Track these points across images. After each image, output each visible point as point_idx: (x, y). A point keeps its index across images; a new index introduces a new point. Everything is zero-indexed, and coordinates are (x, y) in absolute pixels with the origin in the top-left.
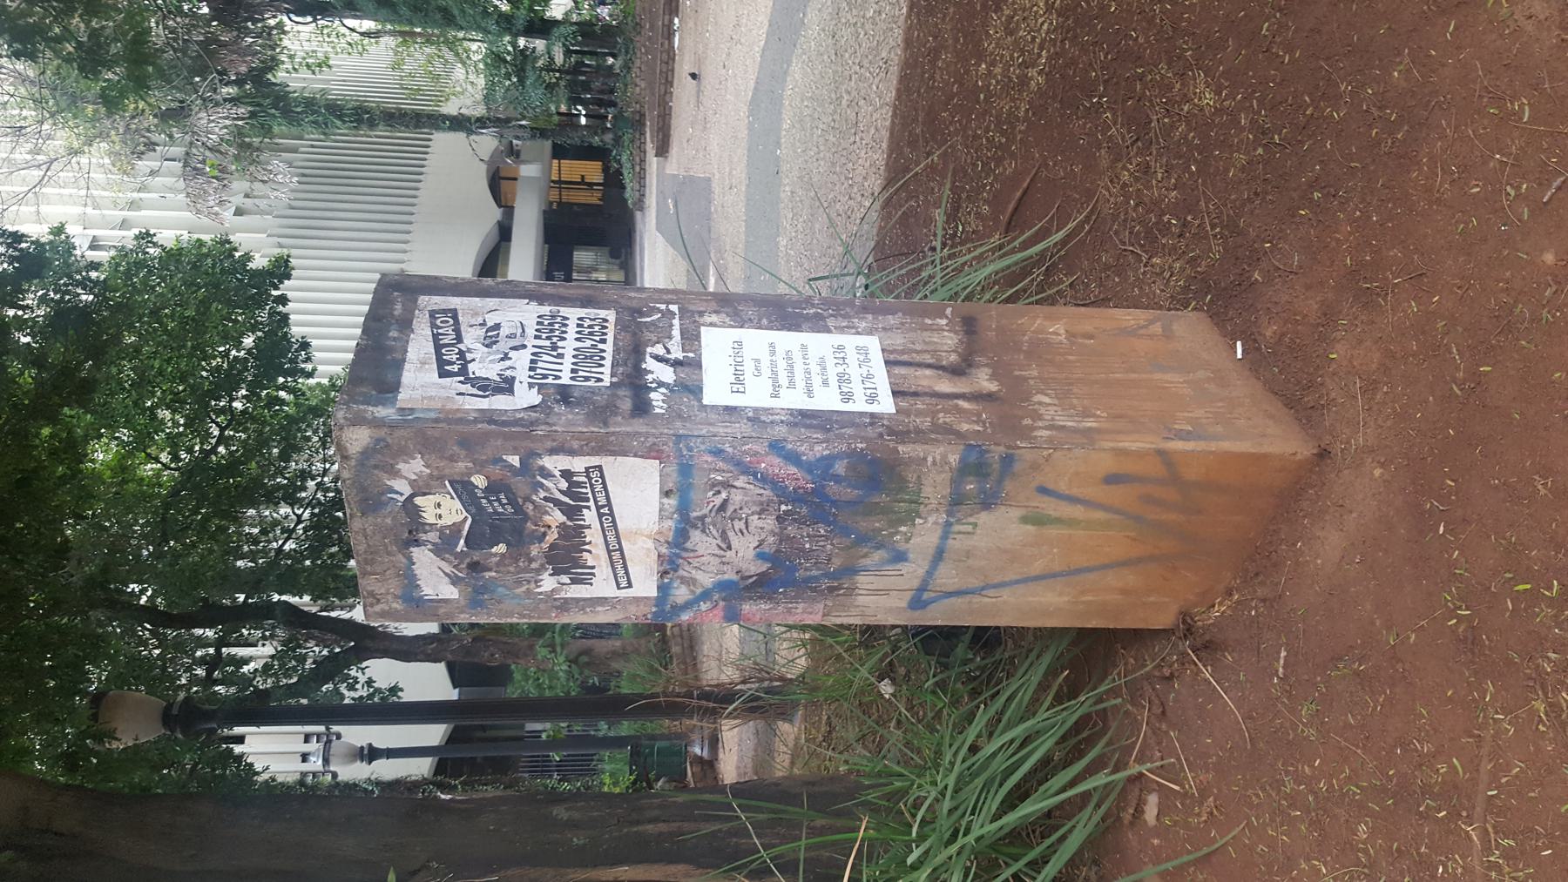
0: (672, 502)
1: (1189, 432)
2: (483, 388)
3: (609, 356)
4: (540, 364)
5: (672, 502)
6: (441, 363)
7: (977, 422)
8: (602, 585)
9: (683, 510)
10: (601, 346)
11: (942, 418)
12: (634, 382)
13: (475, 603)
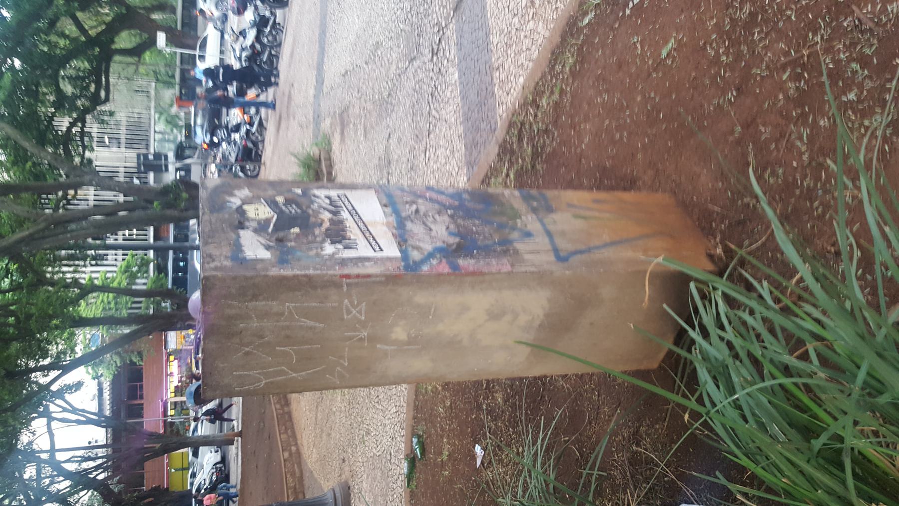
8: (363, 250)
9: (396, 212)
13: (282, 261)
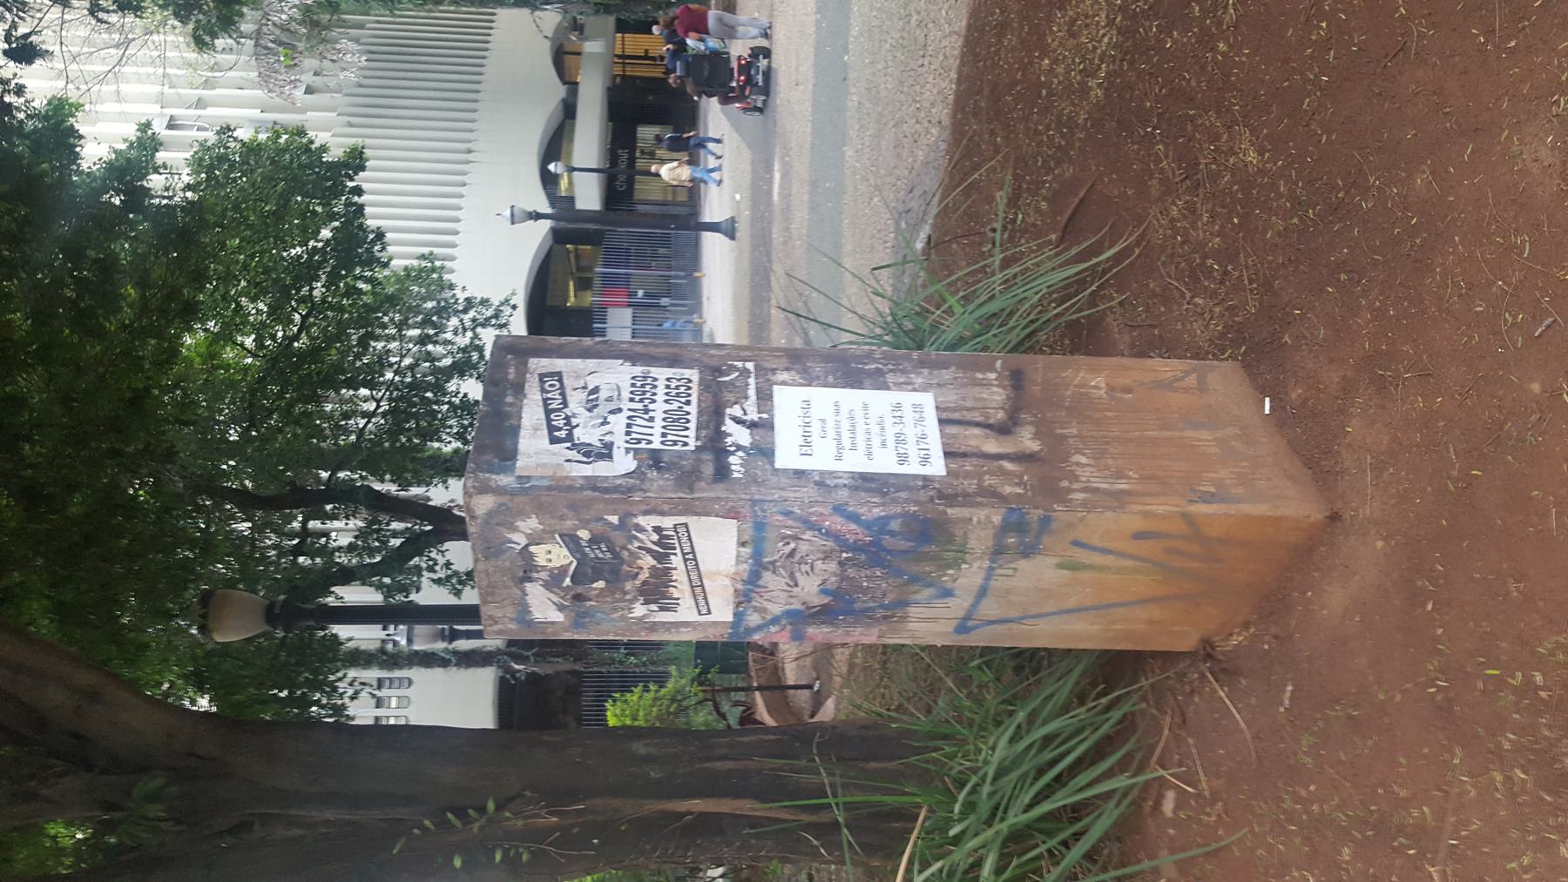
0: (747, 550)
1: (1212, 495)
2: (587, 454)
3: (693, 418)
4: (635, 429)
5: (747, 550)
6: (552, 429)
7: (1018, 485)
8: (686, 611)
9: (757, 556)
10: (686, 408)
11: (988, 481)
12: (715, 444)
13: (577, 624)
